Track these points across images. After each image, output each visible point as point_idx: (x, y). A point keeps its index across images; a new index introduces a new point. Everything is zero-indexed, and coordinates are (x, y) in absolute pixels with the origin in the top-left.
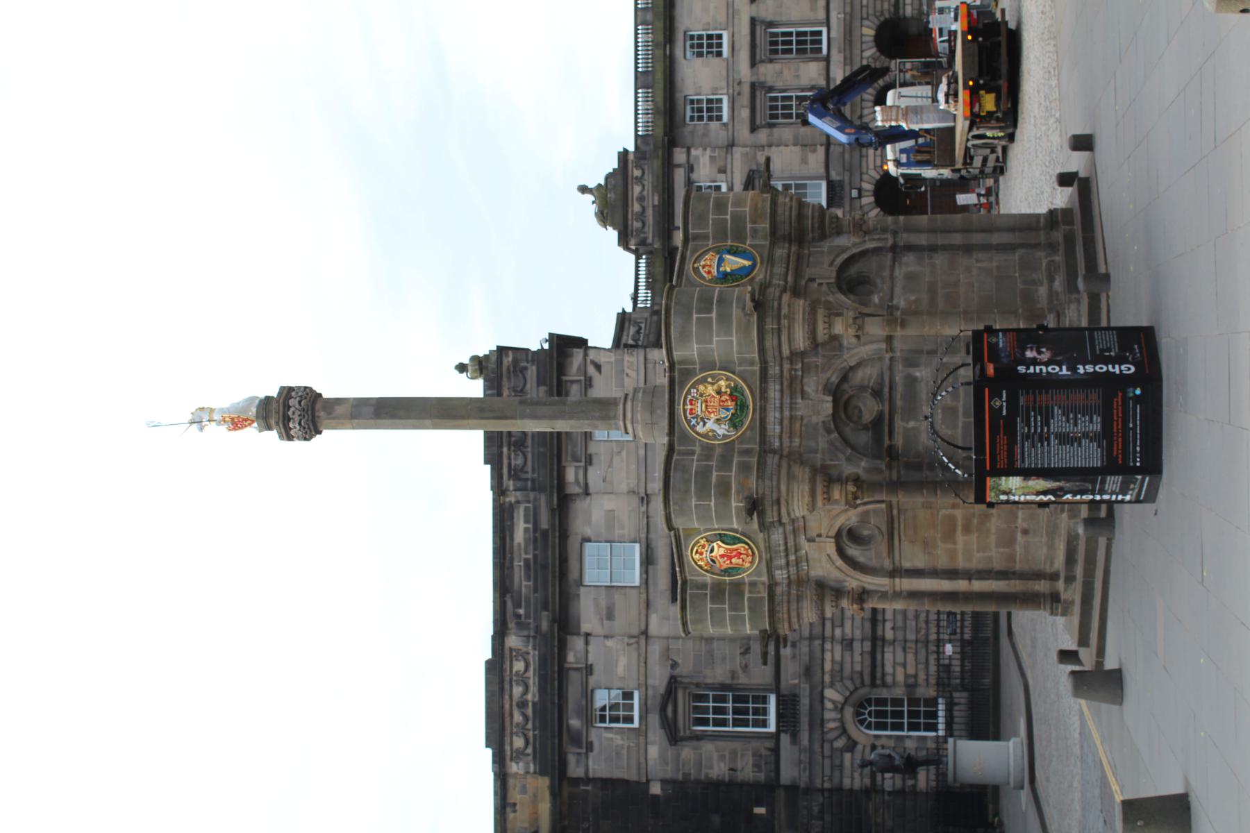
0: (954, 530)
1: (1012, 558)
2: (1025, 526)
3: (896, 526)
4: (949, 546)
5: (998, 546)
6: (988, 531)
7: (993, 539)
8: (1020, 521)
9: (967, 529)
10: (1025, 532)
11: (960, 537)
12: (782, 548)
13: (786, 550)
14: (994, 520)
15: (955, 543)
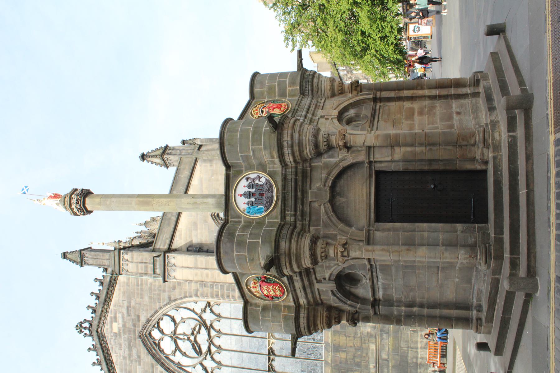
0: (413, 114)
1: (452, 127)
2: (458, 110)
3: (377, 114)
4: (409, 122)
5: (442, 120)
6: (435, 114)
7: (438, 118)
8: (454, 108)
9: (421, 113)
10: (458, 113)
11: (417, 118)
12: (306, 107)
13: (308, 109)
14: (438, 108)
15: (413, 121)
